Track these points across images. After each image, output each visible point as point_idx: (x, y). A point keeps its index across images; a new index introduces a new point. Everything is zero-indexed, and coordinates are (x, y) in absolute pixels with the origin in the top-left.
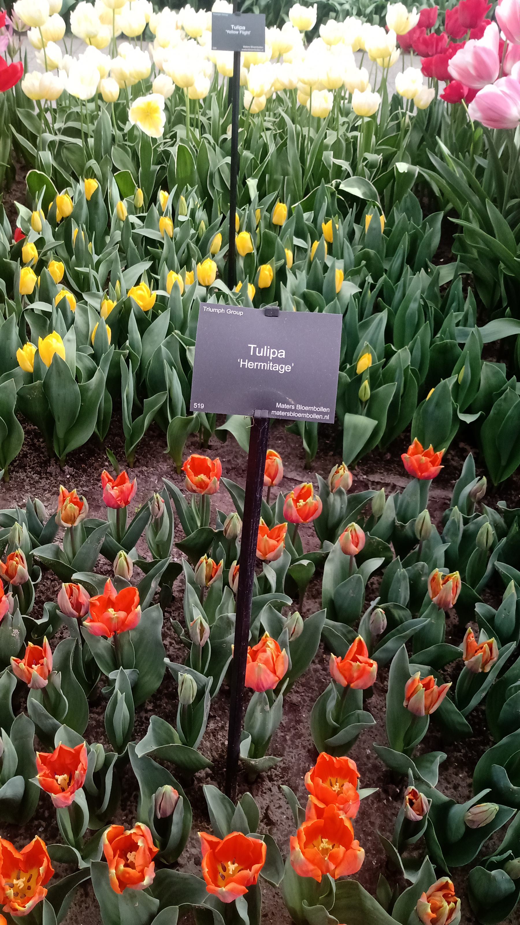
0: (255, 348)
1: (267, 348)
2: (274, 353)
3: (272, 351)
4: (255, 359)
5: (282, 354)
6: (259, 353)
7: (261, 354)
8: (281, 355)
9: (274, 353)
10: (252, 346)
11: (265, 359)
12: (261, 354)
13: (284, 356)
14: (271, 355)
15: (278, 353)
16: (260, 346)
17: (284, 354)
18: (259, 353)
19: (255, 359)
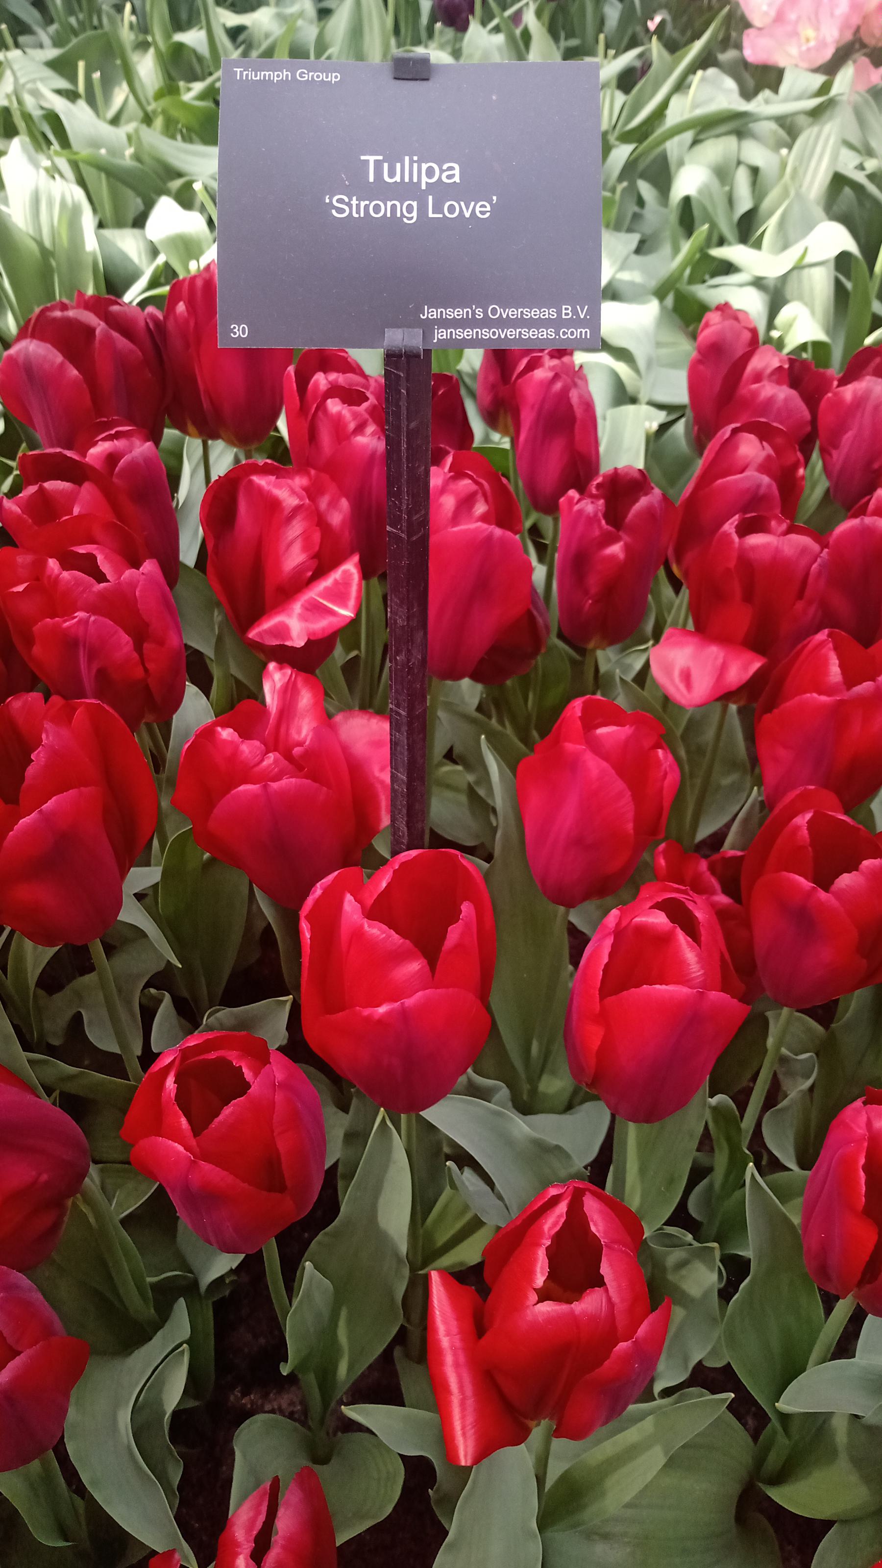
0: (378, 165)
1: (412, 162)
2: (430, 173)
3: (424, 166)
4: (382, 191)
6: (392, 174)
7: (398, 178)
8: (449, 177)
9: (430, 173)
10: (372, 159)
12: (398, 178)
14: (424, 179)
15: (442, 171)
16: (393, 159)
18: (392, 174)
19: (382, 191)
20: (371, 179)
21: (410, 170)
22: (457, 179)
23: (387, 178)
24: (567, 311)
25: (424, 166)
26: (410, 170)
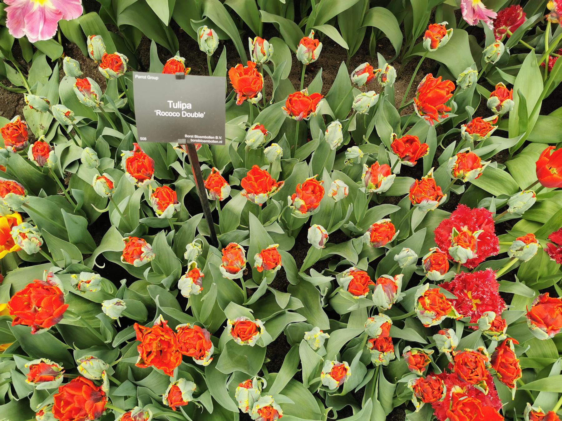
0: (172, 103)
2: (184, 106)
4: (173, 110)
5: (189, 106)
6: (175, 106)
9: (184, 106)
10: (170, 102)
11: (180, 110)
13: (191, 108)
16: (175, 102)
18: (175, 106)
19: (173, 110)
20: (170, 107)
21: (179, 105)
22: (191, 108)
23: (174, 107)
24: (217, 138)
25: (183, 104)
26: (179, 105)
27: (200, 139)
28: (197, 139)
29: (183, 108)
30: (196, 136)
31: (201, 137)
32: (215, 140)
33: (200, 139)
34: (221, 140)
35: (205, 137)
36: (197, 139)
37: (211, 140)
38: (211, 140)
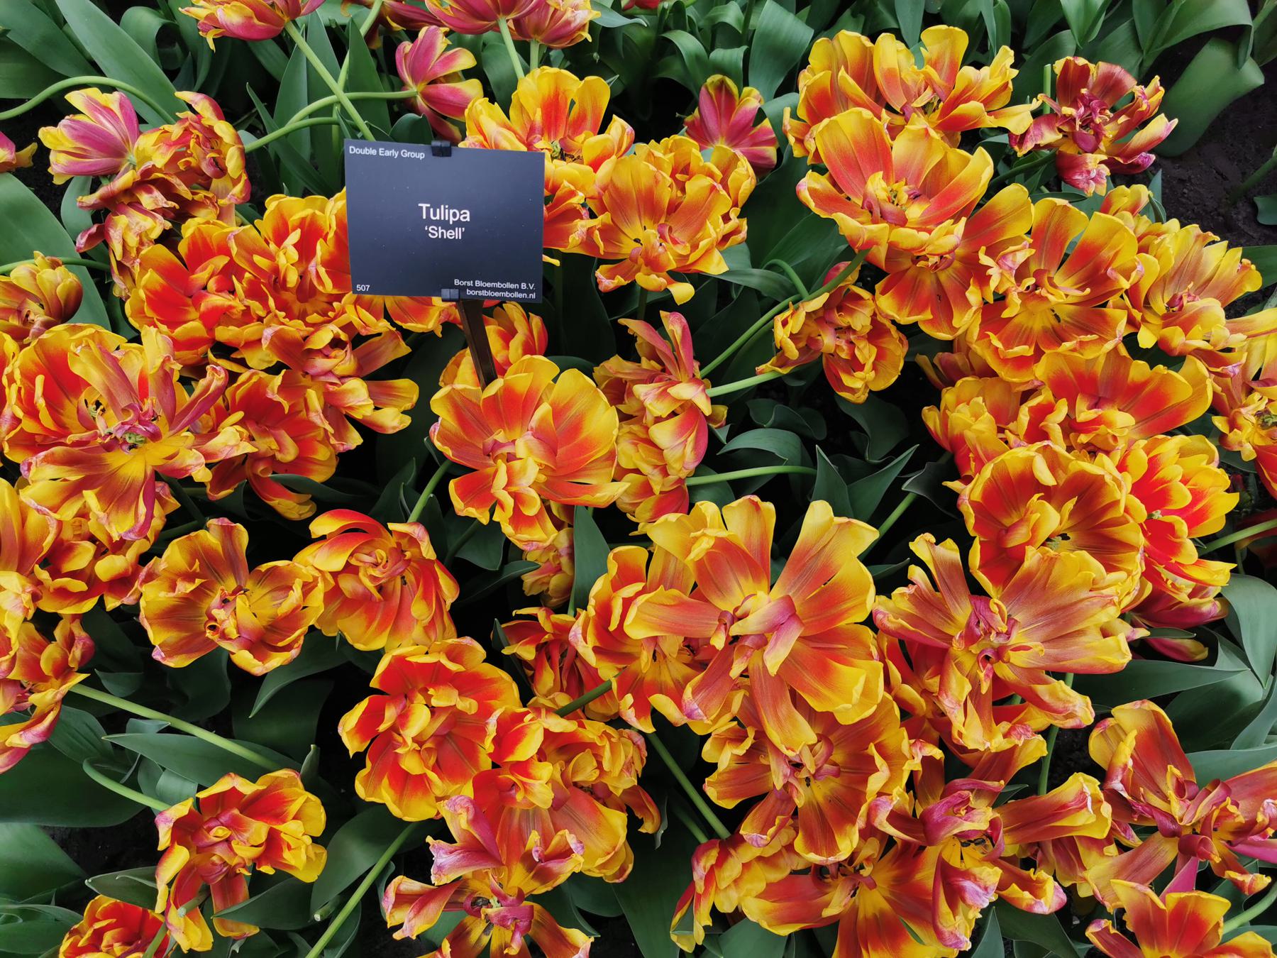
0: (428, 209)
2: (454, 215)
5: (466, 216)
9: (454, 215)
10: (424, 206)
11: (445, 225)
14: (452, 219)
16: (436, 206)
17: (468, 215)
19: (429, 222)
21: (444, 213)
26: (444, 213)
27: (487, 289)
28: (481, 289)
29: (452, 219)
30: (478, 283)
31: (488, 285)
32: (520, 291)
33: (487, 289)
34: (532, 292)
35: (498, 285)
36: (481, 289)
37: (510, 290)
38: (510, 290)
